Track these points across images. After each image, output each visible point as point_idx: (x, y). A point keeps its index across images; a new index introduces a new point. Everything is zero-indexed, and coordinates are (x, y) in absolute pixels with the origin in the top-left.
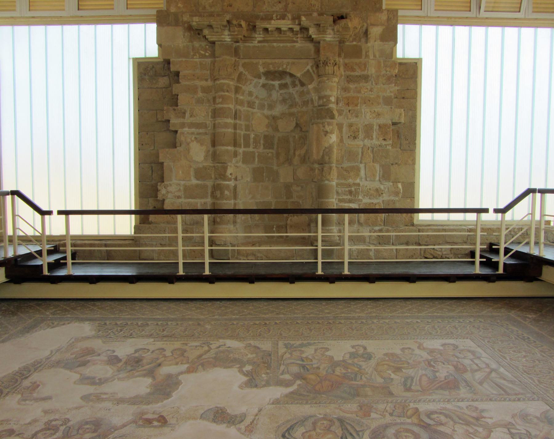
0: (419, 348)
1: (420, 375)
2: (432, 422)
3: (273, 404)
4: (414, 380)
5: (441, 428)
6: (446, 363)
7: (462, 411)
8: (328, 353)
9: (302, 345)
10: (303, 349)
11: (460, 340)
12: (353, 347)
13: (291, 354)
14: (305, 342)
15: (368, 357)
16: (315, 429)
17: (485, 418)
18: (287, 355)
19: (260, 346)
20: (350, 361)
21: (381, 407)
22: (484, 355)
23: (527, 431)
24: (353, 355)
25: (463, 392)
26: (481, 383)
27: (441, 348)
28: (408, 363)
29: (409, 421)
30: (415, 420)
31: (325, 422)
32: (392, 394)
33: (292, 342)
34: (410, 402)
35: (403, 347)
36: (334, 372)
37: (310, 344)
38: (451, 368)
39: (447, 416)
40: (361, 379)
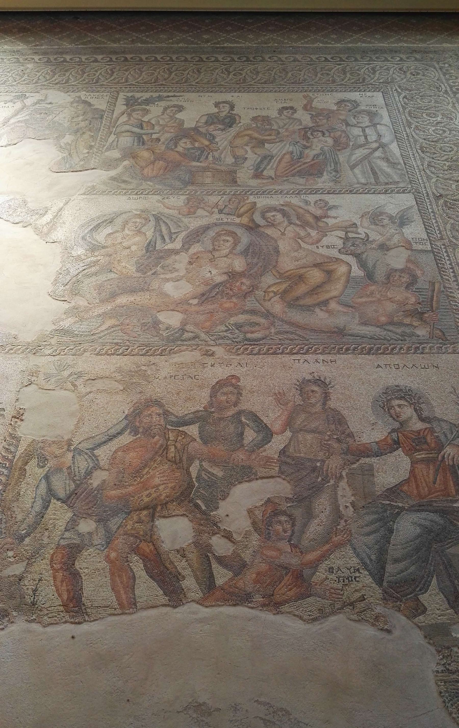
0: (305, 108)
1: (284, 152)
2: (262, 222)
3: (84, 194)
4: (273, 161)
5: (269, 231)
6: (327, 134)
7: (306, 208)
8: (179, 116)
9: (148, 102)
10: (148, 107)
11: (368, 94)
12: (217, 105)
14: (155, 95)
15: (230, 121)
17: (328, 217)
18: (124, 118)
19: (92, 101)
20: (203, 130)
21: (213, 199)
22: (386, 119)
24: (212, 120)
25: (324, 181)
26: (352, 168)
27: (335, 108)
28: (279, 133)
29: (238, 220)
30: (245, 220)
31: (138, 220)
32: (236, 182)
33: (137, 95)
34: (251, 194)
35: (285, 105)
36: (176, 147)
37: (160, 98)
38: (330, 141)
39: (285, 214)
40: (207, 157)
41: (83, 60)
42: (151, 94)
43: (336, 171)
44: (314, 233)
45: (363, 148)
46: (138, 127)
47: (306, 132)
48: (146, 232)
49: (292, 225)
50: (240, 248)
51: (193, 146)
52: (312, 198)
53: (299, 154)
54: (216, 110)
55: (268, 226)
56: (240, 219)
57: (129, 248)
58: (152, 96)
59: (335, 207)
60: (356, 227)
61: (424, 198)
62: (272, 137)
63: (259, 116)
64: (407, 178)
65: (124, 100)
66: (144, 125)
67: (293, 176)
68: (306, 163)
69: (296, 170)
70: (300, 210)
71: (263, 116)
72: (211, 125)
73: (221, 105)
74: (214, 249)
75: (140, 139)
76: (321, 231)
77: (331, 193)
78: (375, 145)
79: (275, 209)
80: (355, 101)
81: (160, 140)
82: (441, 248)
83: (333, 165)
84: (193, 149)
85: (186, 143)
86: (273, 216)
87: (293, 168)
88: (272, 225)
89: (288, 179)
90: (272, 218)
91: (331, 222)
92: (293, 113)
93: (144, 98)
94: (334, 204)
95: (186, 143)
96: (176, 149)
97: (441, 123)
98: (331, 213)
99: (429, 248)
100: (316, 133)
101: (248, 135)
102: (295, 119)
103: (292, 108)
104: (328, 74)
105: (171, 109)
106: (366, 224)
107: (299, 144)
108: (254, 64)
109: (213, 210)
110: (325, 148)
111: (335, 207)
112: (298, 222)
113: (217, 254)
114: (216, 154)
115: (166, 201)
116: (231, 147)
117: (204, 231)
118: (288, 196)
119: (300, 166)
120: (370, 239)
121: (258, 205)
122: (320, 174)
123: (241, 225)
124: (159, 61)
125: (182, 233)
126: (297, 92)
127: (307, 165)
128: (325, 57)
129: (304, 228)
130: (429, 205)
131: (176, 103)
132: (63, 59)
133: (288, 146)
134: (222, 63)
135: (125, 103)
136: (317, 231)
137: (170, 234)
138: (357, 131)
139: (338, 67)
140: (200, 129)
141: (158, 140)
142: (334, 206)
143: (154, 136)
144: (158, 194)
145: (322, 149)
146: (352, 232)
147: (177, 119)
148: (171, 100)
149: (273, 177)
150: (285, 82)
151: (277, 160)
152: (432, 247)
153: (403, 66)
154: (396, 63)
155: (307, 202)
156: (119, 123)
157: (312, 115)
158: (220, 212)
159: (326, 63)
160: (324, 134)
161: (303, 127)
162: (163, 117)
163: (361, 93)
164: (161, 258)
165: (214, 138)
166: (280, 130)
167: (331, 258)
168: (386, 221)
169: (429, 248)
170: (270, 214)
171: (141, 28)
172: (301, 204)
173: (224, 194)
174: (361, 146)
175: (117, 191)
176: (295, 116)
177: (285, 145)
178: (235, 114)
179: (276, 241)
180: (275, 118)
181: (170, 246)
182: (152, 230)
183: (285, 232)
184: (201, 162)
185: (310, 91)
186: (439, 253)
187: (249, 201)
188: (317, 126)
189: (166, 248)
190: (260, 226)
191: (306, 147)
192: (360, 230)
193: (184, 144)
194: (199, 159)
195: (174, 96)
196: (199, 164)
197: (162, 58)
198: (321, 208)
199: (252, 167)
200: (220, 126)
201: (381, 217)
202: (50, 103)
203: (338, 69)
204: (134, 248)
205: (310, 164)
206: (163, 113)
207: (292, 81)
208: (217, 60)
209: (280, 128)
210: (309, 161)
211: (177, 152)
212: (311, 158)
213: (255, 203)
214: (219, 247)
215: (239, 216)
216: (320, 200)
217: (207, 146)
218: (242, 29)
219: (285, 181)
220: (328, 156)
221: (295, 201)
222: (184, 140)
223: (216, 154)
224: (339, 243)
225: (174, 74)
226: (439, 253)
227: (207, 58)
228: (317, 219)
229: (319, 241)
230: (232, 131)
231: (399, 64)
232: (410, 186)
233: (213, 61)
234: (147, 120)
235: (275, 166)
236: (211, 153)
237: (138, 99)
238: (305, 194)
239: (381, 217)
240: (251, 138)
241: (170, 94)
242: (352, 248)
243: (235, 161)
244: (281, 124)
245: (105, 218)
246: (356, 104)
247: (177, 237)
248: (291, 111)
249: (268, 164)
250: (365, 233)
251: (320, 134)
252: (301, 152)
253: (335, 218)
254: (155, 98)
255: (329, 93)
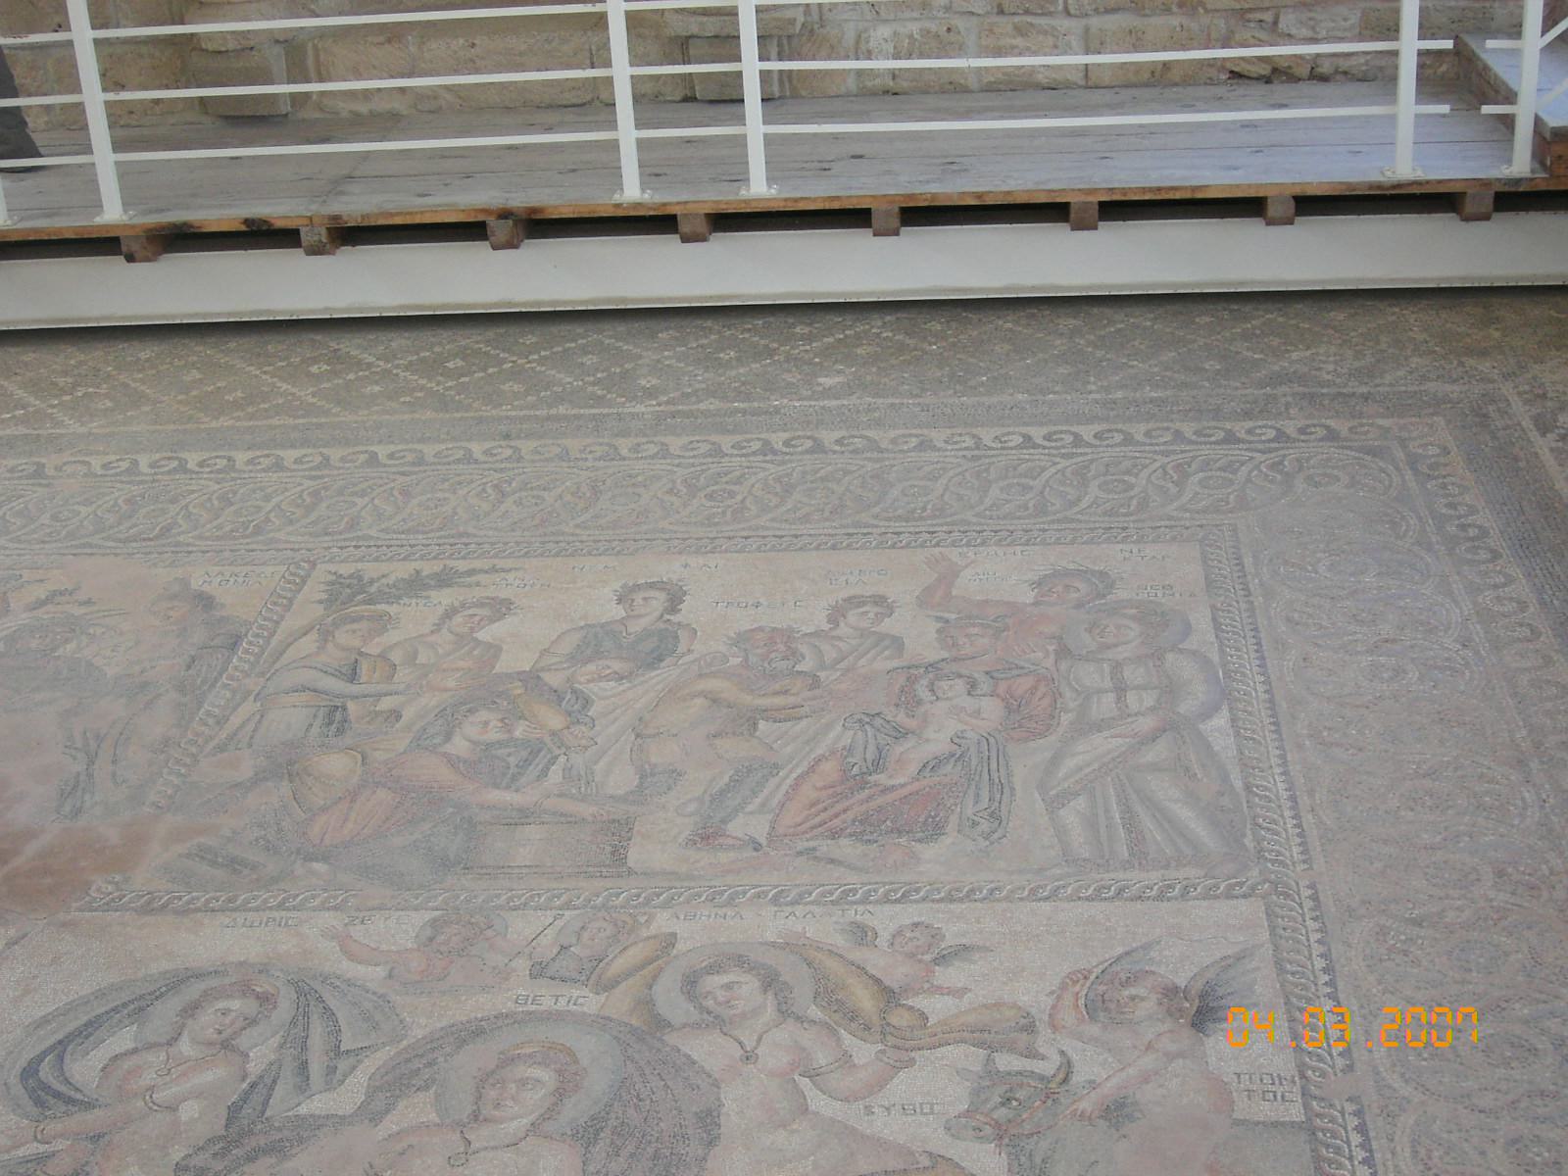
6: (985, 686)
7: (857, 955)
13: (326, 635)
16: (173, 1041)
17: (939, 990)
23: (1067, 1068)
29: (590, 1003)
31: (236, 1004)
33: (370, 570)
34: (666, 905)
36: (448, 737)
38: (992, 710)
39: (770, 981)
40: (545, 772)
41: (239, 465)
42: (417, 565)
43: (995, 816)
44: (864, 1052)
45: (1106, 733)
46: (337, 674)
47: (912, 680)
48: (251, 1049)
49: (791, 1021)
50: (576, 1109)
51: (506, 736)
52: (885, 920)
53: (870, 756)
54: (619, 612)
55: (697, 1026)
56: (603, 998)
57: (172, 1108)
58: (418, 572)
59: (963, 951)
60: (1030, 1028)
61: (1303, 915)
62: (791, 700)
63: (761, 629)
64: (1249, 842)
65: (323, 587)
66: (364, 667)
67: (834, 835)
68: (893, 788)
69: (850, 815)
70: (832, 964)
71: (774, 629)
72: (589, 660)
73: (638, 597)
74: (476, 1116)
75: (335, 717)
76: (895, 1047)
77: (961, 900)
78: (1146, 724)
79: (741, 962)
80: (1102, 574)
81: (399, 717)
82: (1342, 1113)
83: (985, 795)
84: (500, 744)
85: (486, 723)
86: (728, 987)
87: (839, 807)
88: (718, 1022)
89: (814, 849)
90: (721, 995)
91: (937, 1007)
92: (879, 618)
93: (391, 580)
94: (964, 941)
95: (486, 723)
96: (448, 748)
97: (1394, 641)
98: (945, 976)
99: (1295, 1113)
100: (944, 684)
101: (703, 694)
102: (882, 637)
103: (879, 600)
104: (1026, 488)
105: (471, 612)
106: (1068, 1017)
107: (878, 722)
108: (783, 463)
109: (513, 964)
110: (969, 734)
111: (963, 951)
112: (815, 1012)
113: (480, 1136)
114: (578, 760)
115: (357, 932)
116: (638, 736)
117: (462, 1043)
118: (799, 910)
119: (870, 798)
120: (1077, 1078)
121: (681, 946)
122: (934, 830)
123: (603, 1022)
124: (476, 461)
125: (378, 1054)
126: (908, 545)
127: (889, 797)
128: (1021, 434)
129: (833, 1032)
130: (1318, 941)
131: (491, 592)
132: (175, 463)
133: (839, 728)
134: (677, 461)
135: (324, 596)
136: (880, 1047)
137: (337, 1051)
138: (1091, 675)
139: (1064, 463)
140: (546, 677)
141: (395, 715)
142: (965, 948)
143: (386, 704)
144: (335, 908)
145: (957, 739)
146: (1012, 1049)
147: (478, 642)
148: (478, 584)
149: (764, 842)
150: (876, 517)
151: (789, 781)
152: (1306, 1106)
153: (1284, 456)
154: (1260, 446)
155: (862, 934)
156: (284, 660)
157: (947, 621)
158: (539, 971)
159: (1025, 454)
160: (972, 685)
161: (905, 664)
162: (432, 638)
163: (1127, 547)
164: (268, 1150)
165: (587, 702)
166: (822, 675)
167: (912, 1153)
168: (1149, 1006)
169: (1295, 1113)
170: (716, 978)
171: (314, 369)
172: (840, 941)
173: (568, 906)
174: (1098, 727)
175: (198, 898)
176: (887, 626)
177: (829, 727)
178: (679, 624)
179: (716, 1084)
180: (816, 634)
181: (316, 1105)
182: (275, 1041)
183: (759, 1051)
184: (517, 791)
185: (953, 544)
186: (1334, 1136)
187: (653, 930)
188: (955, 660)
189: (303, 1110)
190: (669, 1025)
191: (901, 734)
192: (1043, 1042)
193: (480, 728)
194: (514, 778)
195: (494, 570)
196: (509, 797)
197: (487, 452)
198: (912, 955)
199: (692, 807)
200: (617, 666)
201: (1133, 991)
202: (89, 602)
203: (1063, 471)
204: (189, 1111)
205: (905, 791)
206: (437, 628)
207: (900, 512)
208: (664, 452)
209: (822, 667)
210: (902, 780)
211: (444, 755)
212: (913, 769)
213: (671, 940)
214: (497, 1106)
215: (608, 986)
216: (916, 925)
217: (553, 734)
218: (771, 356)
219: (800, 853)
220: (974, 762)
221: (822, 927)
222: (483, 715)
223: (578, 760)
224: (956, 1097)
225: (510, 500)
226: (1334, 1136)
227: (636, 448)
228: (889, 996)
229: (881, 1083)
230: (654, 681)
231: (1270, 451)
232: (1255, 872)
233: (652, 457)
234: (375, 651)
235: (774, 802)
236: (562, 759)
237: (372, 582)
238: (865, 901)
239: (1133, 991)
240: (715, 700)
241: (477, 564)
242: (1002, 1113)
243: (640, 786)
244: (830, 653)
245: (125, 997)
246: (1105, 581)
247: (354, 1068)
248: (872, 610)
249: (754, 793)
250: (1062, 1053)
251: (960, 685)
252: (880, 750)
253: (959, 993)
254: (427, 576)
255: (1019, 549)
